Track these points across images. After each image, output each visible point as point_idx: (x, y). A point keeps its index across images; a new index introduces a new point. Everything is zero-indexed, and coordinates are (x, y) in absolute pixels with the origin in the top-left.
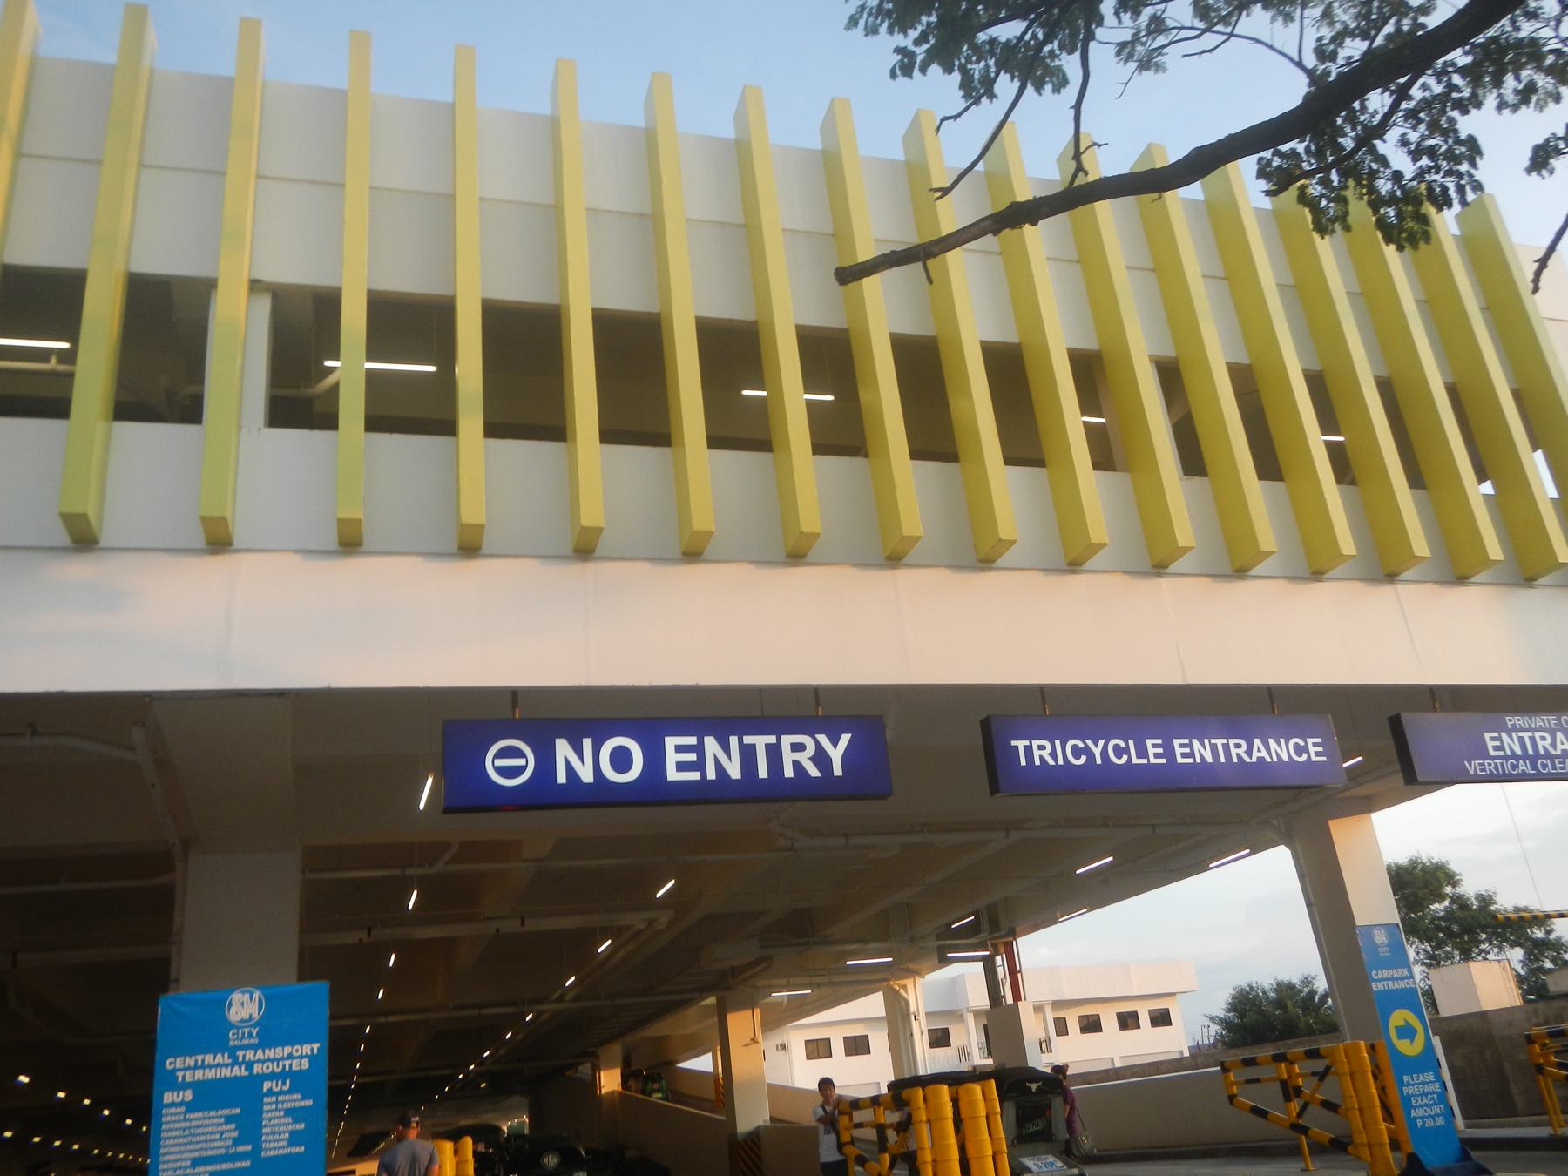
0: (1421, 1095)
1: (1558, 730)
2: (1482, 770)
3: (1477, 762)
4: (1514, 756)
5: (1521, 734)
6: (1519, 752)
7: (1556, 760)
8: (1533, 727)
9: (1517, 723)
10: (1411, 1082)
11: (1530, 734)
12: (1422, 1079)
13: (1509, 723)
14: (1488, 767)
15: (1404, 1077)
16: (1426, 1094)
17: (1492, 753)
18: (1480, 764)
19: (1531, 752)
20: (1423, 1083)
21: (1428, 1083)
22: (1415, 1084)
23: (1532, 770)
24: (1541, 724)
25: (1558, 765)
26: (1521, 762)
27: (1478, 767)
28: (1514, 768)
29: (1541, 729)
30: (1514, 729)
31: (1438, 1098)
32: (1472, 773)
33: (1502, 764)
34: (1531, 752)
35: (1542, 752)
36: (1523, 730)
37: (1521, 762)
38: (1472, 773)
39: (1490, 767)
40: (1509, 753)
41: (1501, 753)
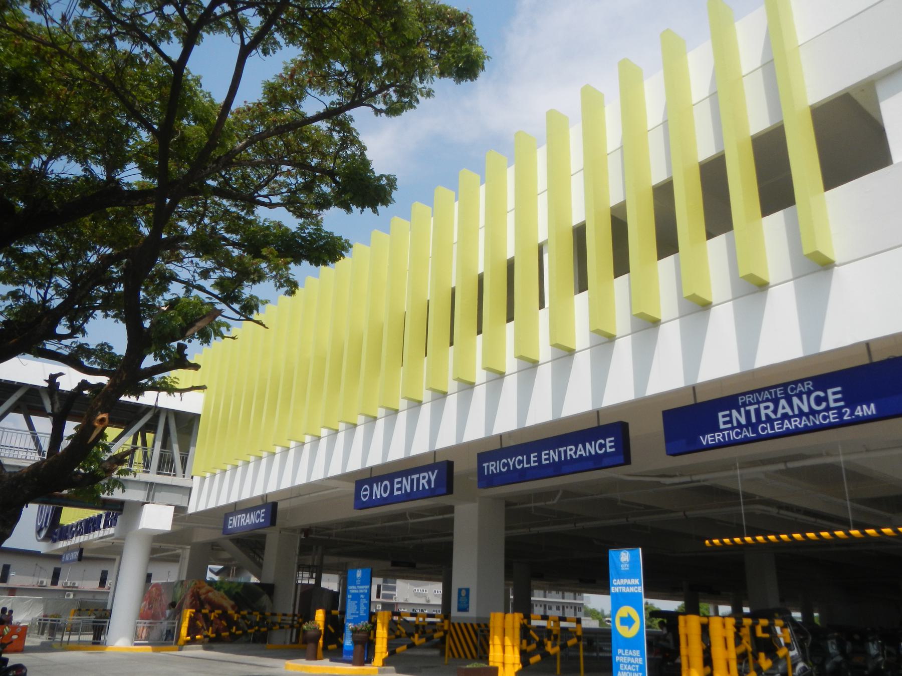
0: (628, 664)
1: (782, 398)
2: (712, 441)
3: (709, 435)
4: (740, 425)
5: (748, 408)
6: (743, 421)
7: (775, 423)
8: (760, 400)
9: (747, 399)
10: (623, 654)
11: (756, 406)
12: (630, 653)
13: (740, 401)
14: (717, 438)
15: (619, 650)
16: (631, 664)
17: (722, 426)
18: (711, 437)
19: (754, 420)
20: (631, 656)
21: (634, 657)
22: (625, 656)
23: (753, 433)
26: (744, 429)
27: (709, 439)
28: (737, 436)
29: (767, 400)
30: (744, 405)
31: (639, 668)
32: (705, 443)
33: (729, 434)
34: (754, 420)
35: (763, 418)
36: (751, 404)
37: (744, 429)
38: (705, 443)
39: (718, 437)
40: (735, 424)
41: (729, 426)
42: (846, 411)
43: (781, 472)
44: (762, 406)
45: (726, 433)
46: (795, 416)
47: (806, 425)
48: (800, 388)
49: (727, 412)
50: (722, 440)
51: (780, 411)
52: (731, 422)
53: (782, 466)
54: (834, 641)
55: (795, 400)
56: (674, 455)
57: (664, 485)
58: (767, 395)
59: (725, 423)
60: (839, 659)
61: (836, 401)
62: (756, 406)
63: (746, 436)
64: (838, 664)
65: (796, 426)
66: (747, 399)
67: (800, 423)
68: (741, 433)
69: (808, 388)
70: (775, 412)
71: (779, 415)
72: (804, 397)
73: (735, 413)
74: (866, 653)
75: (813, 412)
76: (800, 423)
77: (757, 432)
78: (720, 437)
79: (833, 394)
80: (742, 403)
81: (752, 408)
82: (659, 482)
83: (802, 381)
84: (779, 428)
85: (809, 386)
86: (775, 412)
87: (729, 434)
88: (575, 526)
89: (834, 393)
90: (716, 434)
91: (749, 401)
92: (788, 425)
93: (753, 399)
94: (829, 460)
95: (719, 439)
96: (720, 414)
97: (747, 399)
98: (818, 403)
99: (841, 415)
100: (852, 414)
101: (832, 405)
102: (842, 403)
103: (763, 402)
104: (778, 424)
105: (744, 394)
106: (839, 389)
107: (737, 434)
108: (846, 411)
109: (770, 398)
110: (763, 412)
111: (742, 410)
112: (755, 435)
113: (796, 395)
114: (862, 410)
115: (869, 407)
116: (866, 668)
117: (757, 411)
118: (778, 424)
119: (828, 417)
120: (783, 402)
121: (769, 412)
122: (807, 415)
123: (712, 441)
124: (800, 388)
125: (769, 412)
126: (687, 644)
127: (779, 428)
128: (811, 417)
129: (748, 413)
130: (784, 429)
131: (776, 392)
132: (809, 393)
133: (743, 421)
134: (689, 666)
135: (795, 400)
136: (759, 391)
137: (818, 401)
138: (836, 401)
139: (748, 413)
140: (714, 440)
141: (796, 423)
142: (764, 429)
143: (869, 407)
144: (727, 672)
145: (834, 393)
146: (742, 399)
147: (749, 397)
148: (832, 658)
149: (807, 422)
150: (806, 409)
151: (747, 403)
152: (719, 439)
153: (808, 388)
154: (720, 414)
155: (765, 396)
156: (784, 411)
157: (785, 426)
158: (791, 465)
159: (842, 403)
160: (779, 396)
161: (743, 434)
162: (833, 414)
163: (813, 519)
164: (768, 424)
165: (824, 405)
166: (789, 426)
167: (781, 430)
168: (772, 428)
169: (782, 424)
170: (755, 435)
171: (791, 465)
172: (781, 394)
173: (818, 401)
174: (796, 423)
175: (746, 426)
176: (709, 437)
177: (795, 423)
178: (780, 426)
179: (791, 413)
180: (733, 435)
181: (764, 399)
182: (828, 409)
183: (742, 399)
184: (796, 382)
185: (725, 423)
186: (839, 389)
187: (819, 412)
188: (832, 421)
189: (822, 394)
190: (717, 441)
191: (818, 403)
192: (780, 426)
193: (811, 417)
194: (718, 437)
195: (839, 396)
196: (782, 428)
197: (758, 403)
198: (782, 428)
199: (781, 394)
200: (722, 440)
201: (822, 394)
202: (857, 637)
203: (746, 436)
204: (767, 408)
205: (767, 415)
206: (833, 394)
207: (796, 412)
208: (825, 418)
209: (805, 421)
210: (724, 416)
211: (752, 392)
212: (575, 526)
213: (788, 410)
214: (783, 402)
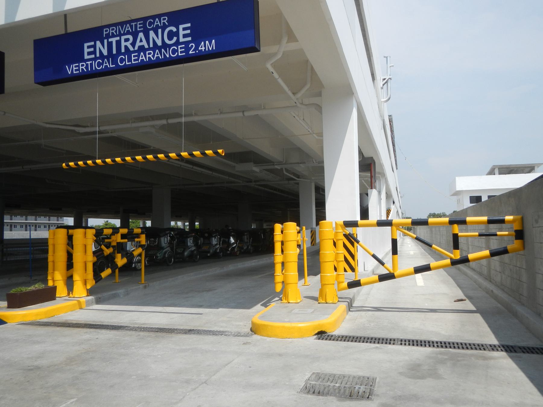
2: (76, 70)
3: (74, 65)
5: (110, 40)
6: (105, 52)
7: (133, 55)
8: (122, 33)
9: (111, 31)
11: (118, 38)
13: (105, 33)
14: (81, 68)
17: (86, 57)
18: (76, 67)
19: (114, 52)
24: (130, 29)
25: (133, 58)
26: (106, 60)
27: (74, 68)
28: (99, 66)
29: (128, 33)
30: (108, 36)
32: (70, 73)
33: (91, 64)
34: (114, 52)
35: (123, 50)
36: (113, 36)
37: (106, 60)
38: (70, 73)
39: (82, 67)
40: (98, 55)
41: (93, 56)
42: (192, 46)
43: (163, 127)
44: (123, 38)
45: (89, 63)
46: (149, 49)
47: (158, 58)
48: (157, 22)
49: (92, 43)
50: (85, 70)
51: (138, 44)
52: (94, 52)
53: (164, 122)
54: (192, 238)
55: (152, 34)
56: (44, 84)
57: (79, 133)
58: (128, 28)
59: (89, 54)
60: (194, 248)
61: (185, 36)
62: (118, 38)
63: (106, 66)
64: (192, 252)
65: (149, 58)
66: (111, 31)
67: (153, 56)
68: (102, 64)
69: (164, 23)
70: (133, 44)
71: (136, 48)
72: (160, 31)
73: (98, 44)
74: (210, 244)
75: (165, 46)
76: (153, 56)
77: (117, 64)
78: (83, 67)
79: (183, 29)
80: (105, 34)
81: (114, 40)
82: (74, 131)
83: (159, 16)
84: (135, 60)
85: (165, 21)
86: (133, 44)
87: (91, 64)
88: (23, 168)
89: (184, 29)
90: (80, 64)
91: (112, 33)
92: (142, 57)
93: (116, 32)
94: (196, 119)
95: (82, 69)
96: (86, 45)
97: (111, 31)
98: (170, 38)
99: (187, 49)
100: (196, 48)
101: (182, 40)
102: (189, 39)
103: (124, 34)
104: (134, 56)
105: (109, 26)
106: (189, 25)
107: (99, 64)
108: (192, 46)
109: (131, 31)
110: (123, 44)
111: (106, 41)
112: (114, 66)
113: (153, 29)
114: (205, 46)
115: (210, 44)
116: (209, 252)
117: (119, 43)
118: (134, 56)
119: (177, 51)
120: (141, 35)
121: (128, 44)
122: (160, 48)
123: (76, 70)
124: (157, 22)
125: (128, 44)
126: (54, 252)
127: (135, 60)
128: (163, 50)
129: (110, 44)
130: (139, 61)
131: (136, 26)
132: (164, 28)
133: (105, 52)
134: (54, 270)
135: (152, 34)
136: (122, 24)
137: (171, 35)
138: (185, 36)
139: (110, 44)
140: (79, 70)
141: (150, 56)
142: (122, 60)
143: (210, 44)
144: (84, 272)
145: (184, 29)
146: (106, 31)
147: (113, 29)
148: (189, 249)
149: (159, 55)
150: (159, 43)
151: (111, 35)
152: (82, 69)
153: (164, 23)
154: (86, 45)
155: (127, 29)
156: (141, 44)
157: (140, 58)
158: (171, 121)
159: (189, 39)
160: (138, 29)
161: (104, 65)
162: (181, 48)
163: (191, 166)
164: (126, 56)
165: (175, 39)
166: (144, 58)
167: (137, 62)
168: (130, 60)
169: (138, 56)
170: (114, 66)
171: (171, 121)
172: (140, 28)
173: (171, 35)
174: (150, 56)
175: (107, 57)
176: (74, 67)
177: (150, 56)
178: (137, 58)
179: (146, 46)
180: (95, 66)
181: (125, 32)
182: (177, 43)
183: (106, 31)
184: (154, 17)
185: (89, 54)
186: (189, 25)
187: (170, 46)
188: (180, 54)
189: (174, 29)
190: (81, 71)
191: (170, 38)
192: (137, 58)
193: (163, 50)
194: (82, 67)
195: (188, 32)
196: (138, 60)
197: (120, 35)
198: (138, 60)
199: (140, 28)
200: (85, 70)
201: (174, 29)
202: (206, 235)
203: (106, 66)
204: (127, 40)
205: (126, 47)
206: (183, 29)
207: (151, 46)
208: (174, 51)
209: (157, 54)
210: (89, 47)
211: (115, 25)
212: (23, 168)
213: (144, 43)
214: (141, 35)
